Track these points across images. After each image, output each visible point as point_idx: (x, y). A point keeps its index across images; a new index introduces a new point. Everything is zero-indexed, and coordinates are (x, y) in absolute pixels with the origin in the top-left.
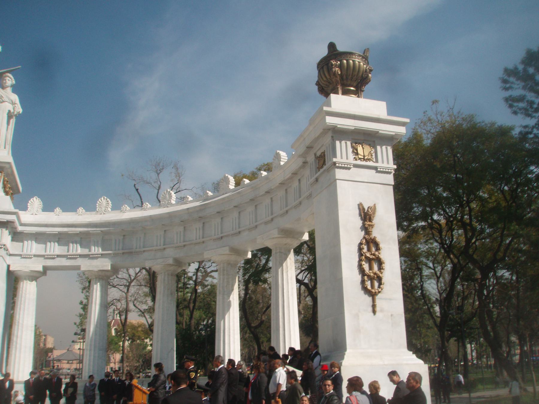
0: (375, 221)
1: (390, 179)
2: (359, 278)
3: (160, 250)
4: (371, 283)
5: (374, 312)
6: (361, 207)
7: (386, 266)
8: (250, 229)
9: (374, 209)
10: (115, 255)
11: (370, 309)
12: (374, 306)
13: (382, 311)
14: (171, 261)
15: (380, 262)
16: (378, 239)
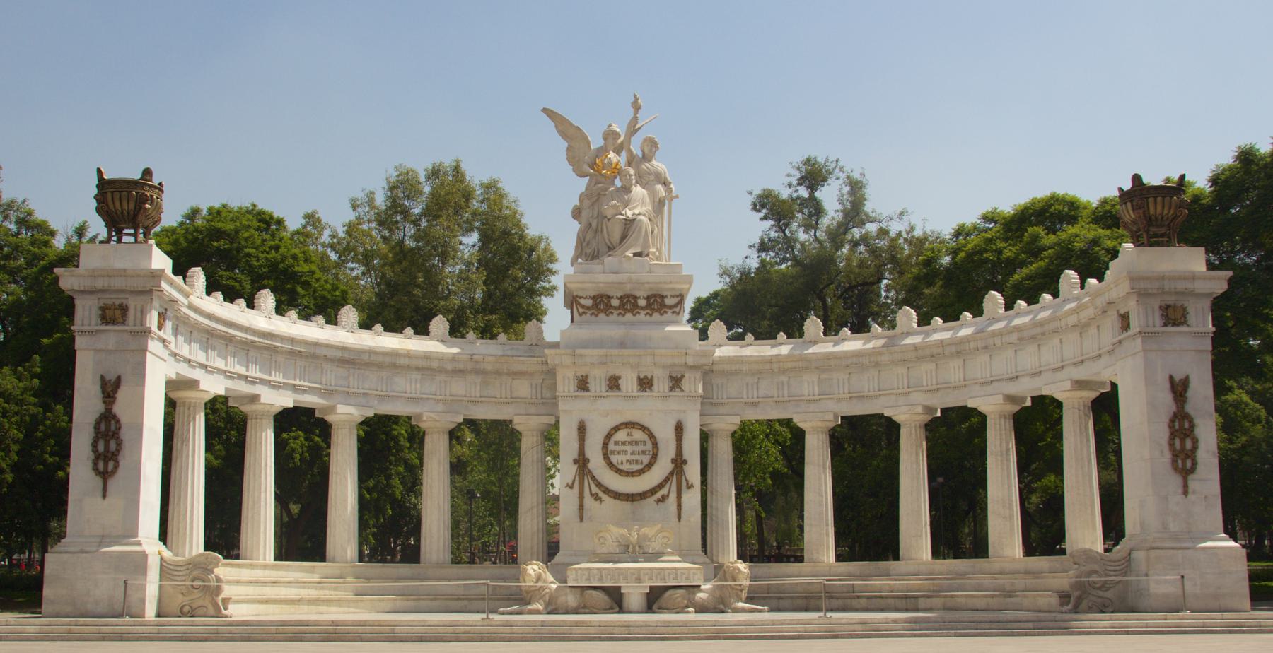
0: (1189, 394)
1: (1208, 344)
2: (1168, 456)
3: (903, 394)
4: (1183, 460)
5: (1186, 493)
6: (1171, 377)
7: (1202, 445)
8: (1032, 375)
9: (1185, 383)
10: (839, 400)
11: (1180, 490)
12: (1185, 486)
13: (1194, 492)
14: (920, 409)
15: (1195, 442)
16: (1192, 413)
